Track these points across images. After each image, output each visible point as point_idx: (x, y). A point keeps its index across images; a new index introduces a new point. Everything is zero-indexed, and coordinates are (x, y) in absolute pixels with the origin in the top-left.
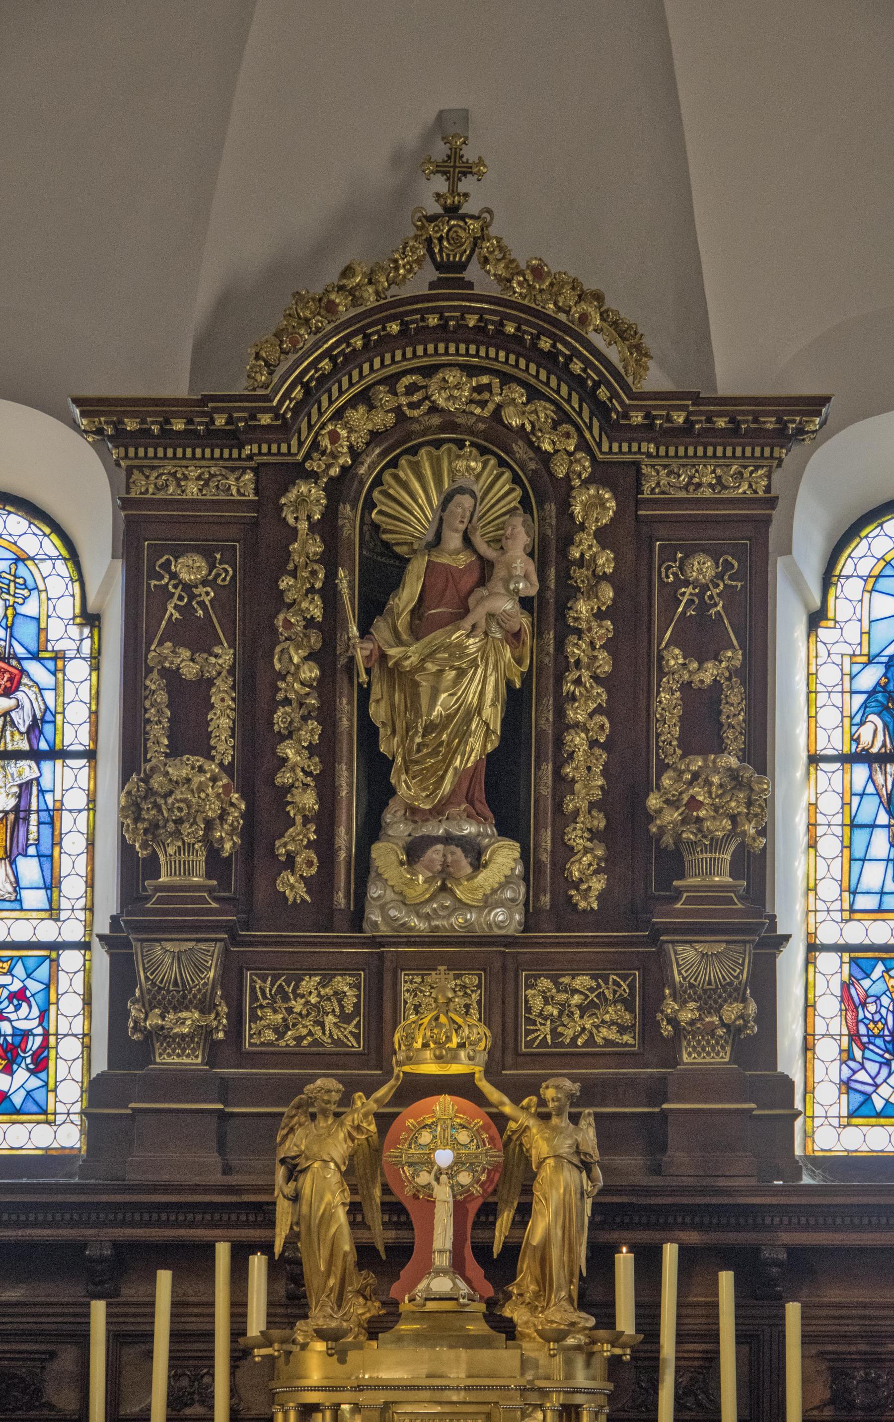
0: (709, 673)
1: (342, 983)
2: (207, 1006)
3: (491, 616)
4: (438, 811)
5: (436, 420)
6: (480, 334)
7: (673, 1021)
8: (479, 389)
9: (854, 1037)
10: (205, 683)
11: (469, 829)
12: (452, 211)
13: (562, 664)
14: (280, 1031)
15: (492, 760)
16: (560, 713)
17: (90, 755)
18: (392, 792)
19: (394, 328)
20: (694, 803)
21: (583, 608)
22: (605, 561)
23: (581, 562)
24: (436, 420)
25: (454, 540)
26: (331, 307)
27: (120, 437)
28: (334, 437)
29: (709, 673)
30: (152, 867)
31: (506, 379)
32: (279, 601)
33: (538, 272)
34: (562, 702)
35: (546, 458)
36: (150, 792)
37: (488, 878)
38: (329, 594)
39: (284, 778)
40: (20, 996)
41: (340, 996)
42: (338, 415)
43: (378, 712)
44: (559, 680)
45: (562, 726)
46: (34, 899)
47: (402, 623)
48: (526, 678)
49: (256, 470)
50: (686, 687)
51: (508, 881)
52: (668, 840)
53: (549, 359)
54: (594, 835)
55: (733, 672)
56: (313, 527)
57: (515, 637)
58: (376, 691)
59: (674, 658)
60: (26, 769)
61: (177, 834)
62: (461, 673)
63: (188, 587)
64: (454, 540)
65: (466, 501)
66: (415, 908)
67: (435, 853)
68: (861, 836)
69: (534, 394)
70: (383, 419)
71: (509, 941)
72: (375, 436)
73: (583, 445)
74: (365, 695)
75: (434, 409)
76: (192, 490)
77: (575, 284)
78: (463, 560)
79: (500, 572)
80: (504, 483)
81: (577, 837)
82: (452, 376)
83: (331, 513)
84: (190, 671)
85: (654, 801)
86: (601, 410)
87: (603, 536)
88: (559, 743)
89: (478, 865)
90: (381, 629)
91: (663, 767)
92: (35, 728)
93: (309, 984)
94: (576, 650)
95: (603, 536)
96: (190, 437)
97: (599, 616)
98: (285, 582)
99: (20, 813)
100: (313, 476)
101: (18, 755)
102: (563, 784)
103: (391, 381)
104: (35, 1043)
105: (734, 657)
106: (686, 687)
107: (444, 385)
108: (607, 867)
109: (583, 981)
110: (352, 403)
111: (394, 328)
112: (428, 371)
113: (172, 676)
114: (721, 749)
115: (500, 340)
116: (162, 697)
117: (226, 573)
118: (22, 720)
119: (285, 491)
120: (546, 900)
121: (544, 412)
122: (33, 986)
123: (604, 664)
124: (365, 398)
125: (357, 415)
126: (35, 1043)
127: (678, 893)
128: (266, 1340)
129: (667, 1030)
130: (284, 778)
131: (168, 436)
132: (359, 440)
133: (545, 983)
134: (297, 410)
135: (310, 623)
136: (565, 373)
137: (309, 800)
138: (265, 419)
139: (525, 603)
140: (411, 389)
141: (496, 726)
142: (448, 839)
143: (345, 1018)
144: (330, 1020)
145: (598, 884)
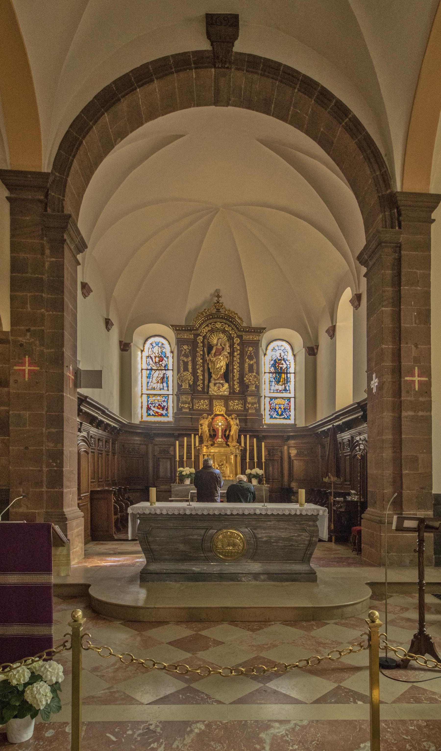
0: (252, 362)
1: (206, 401)
2: (189, 404)
3: (224, 355)
4: (218, 379)
5: (216, 329)
6: (222, 318)
7: (248, 407)
8: (222, 325)
9: (270, 408)
10: (188, 362)
11: (222, 382)
12: (218, 302)
13: (233, 361)
14: (198, 407)
15: (224, 373)
16: (233, 367)
17: (172, 370)
18: (212, 377)
19: (211, 317)
20: (250, 379)
21: (236, 354)
23: (235, 348)
24: (216, 329)
25: (219, 345)
26: (203, 314)
27: (176, 330)
28: (204, 331)
29: (252, 362)
30: (182, 386)
31: (225, 324)
33: (229, 311)
34: (233, 366)
35: (231, 334)
36: (181, 376)
37: (224, 388)
38: (203, 351)
40: (164, 401)
41: (206, 403)
42: (204, 328)
43: (210, 366)
44: (233, 363)
45: (233, 369)
46: (166, 388)
47: (213, 355)
48: (229, 362)
49: (194, 334)
51: (227, 389)
52: (247, 384)
53: (231, 322)
54: (238, 383)
55: (255, 362)
56: (201, 342)
57: (227, 357)
58: (210, 364)
59: (247, 360)
60: (164, 372)
61: (185, 382)
62: (220, 362)
63: (185, 349)
64: (219, 345)
65: (221, 340)
66: (215, 392)
67: (218, 385)
68: (271, 383)
69: (229, 326)
70: (210, 328)
71: (227, 396)
72: (209, 331)
73: (235, 333)
74: (208, 364)
75: (216, 327)
76: (185, 337)
77: (234, 312)
78: (220, 347)
79: (225, 349)
80: (225, 337)
81: (235, 383)
82: (218, 323)
83: (203, 340)
84: (186, 360)
85: (245, 379)
86: (237, 328)
88: (233, 371)
89: (223, 386)
90: (210, 355)
92: (165, 366)
93: (202, 401)
94: (235, 359)
96: (185, 330)
98: (198, 349)
99: (163, 378)
101: (163, 370)
103: (211, 324)
104: (166, 407)
106: (249, 364)
107: (217, 324)
109: (236, 401)
110: (206, 326)
111: (211, 317)
112: (215, 322)
113: (183, 361)
115: (224, 319)
116: (182, 364)
117: (190, 348)
118: (163, 365)
119: (197, 337)
120: (232, 391)
121: (230, 328)
122: (166, 400)
123: (238, 361)
124: (207, 326)
125: (206, 328)
126: (166, 407)
127: (248, 390)
129: (247, 408)
131: (182, 330)
132: (207, 331)
133: (232, 401)
134: (199, 327)
135: (201, 354)
136: (233, 323)
137: (201, 377)
138: (195, 328)
140: (213, 325)
141: (225, 369)
142: (219, 383)
143: (207, 405)
144: (205, 406)
145: (238, 389)
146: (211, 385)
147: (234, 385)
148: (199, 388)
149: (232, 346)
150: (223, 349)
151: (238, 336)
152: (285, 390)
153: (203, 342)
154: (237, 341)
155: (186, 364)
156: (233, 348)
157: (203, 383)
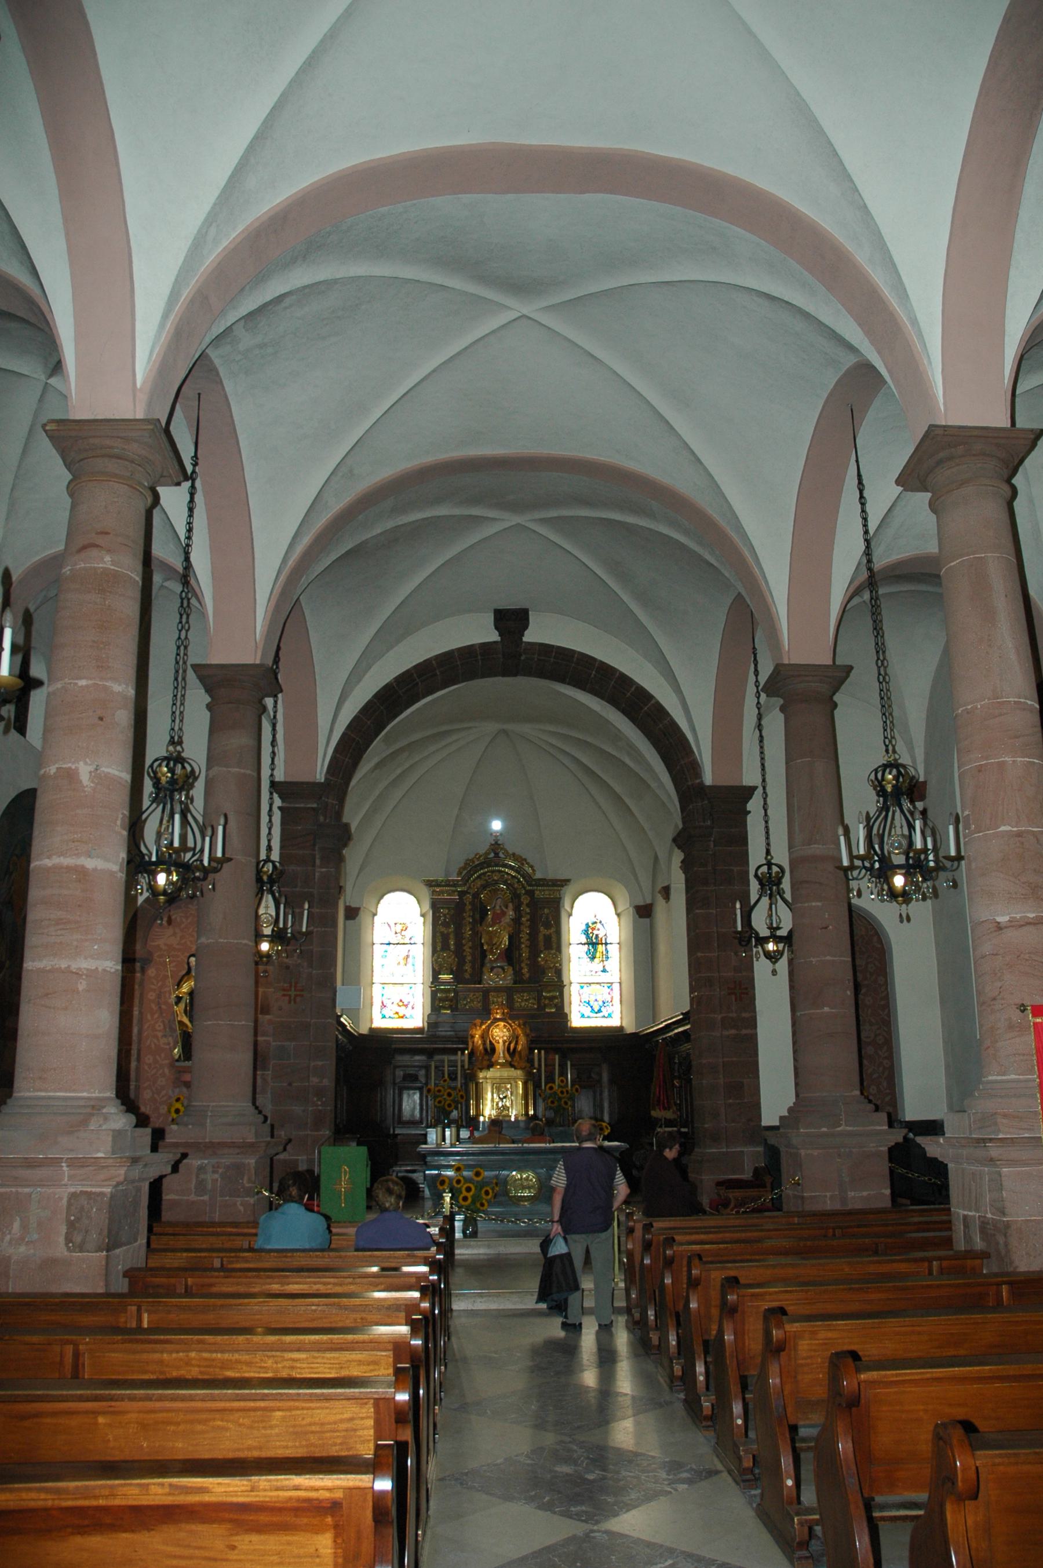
4: (496, 960)
14: (465, 1005)
16: (520, 941)
22: (528, 910)
32: (464, 918)
35: (515, 889)
38: (473, 917)
39: (465, 954)
45: (521, 943)
50: (544, 935)
54: (527, 964)
57: (510, 926)
67: (495, 970)
70: (483, 882)
75: (494, 880)
81: (523, 965)
82: (497, 874)
84: (446, 932)
87: (528, 905)
91: (541, 952)
95: (528, 905)
97: (527, 921)
100: (469, 893)
102: (520, 955)
105: (553, 930)
108: (529, 971)
113: (442, 934)
114: (552, 949)
128: (468, 1069)
130: (465, 954)
132: (479, 886)
135: (470, 923)
139: (513, 920)
142: (498, 967)
145: (527, 975)
146: (485, 970)
147: (521, 969)
148: (467, 976)
149: (517, 909)
150: (504, 914)
151: (528, 893)
152: (604, 971)
153: (472, 903)
154: (525, 900)
155: (445, 938)
156: (520, 911)
157: (473, 967)
